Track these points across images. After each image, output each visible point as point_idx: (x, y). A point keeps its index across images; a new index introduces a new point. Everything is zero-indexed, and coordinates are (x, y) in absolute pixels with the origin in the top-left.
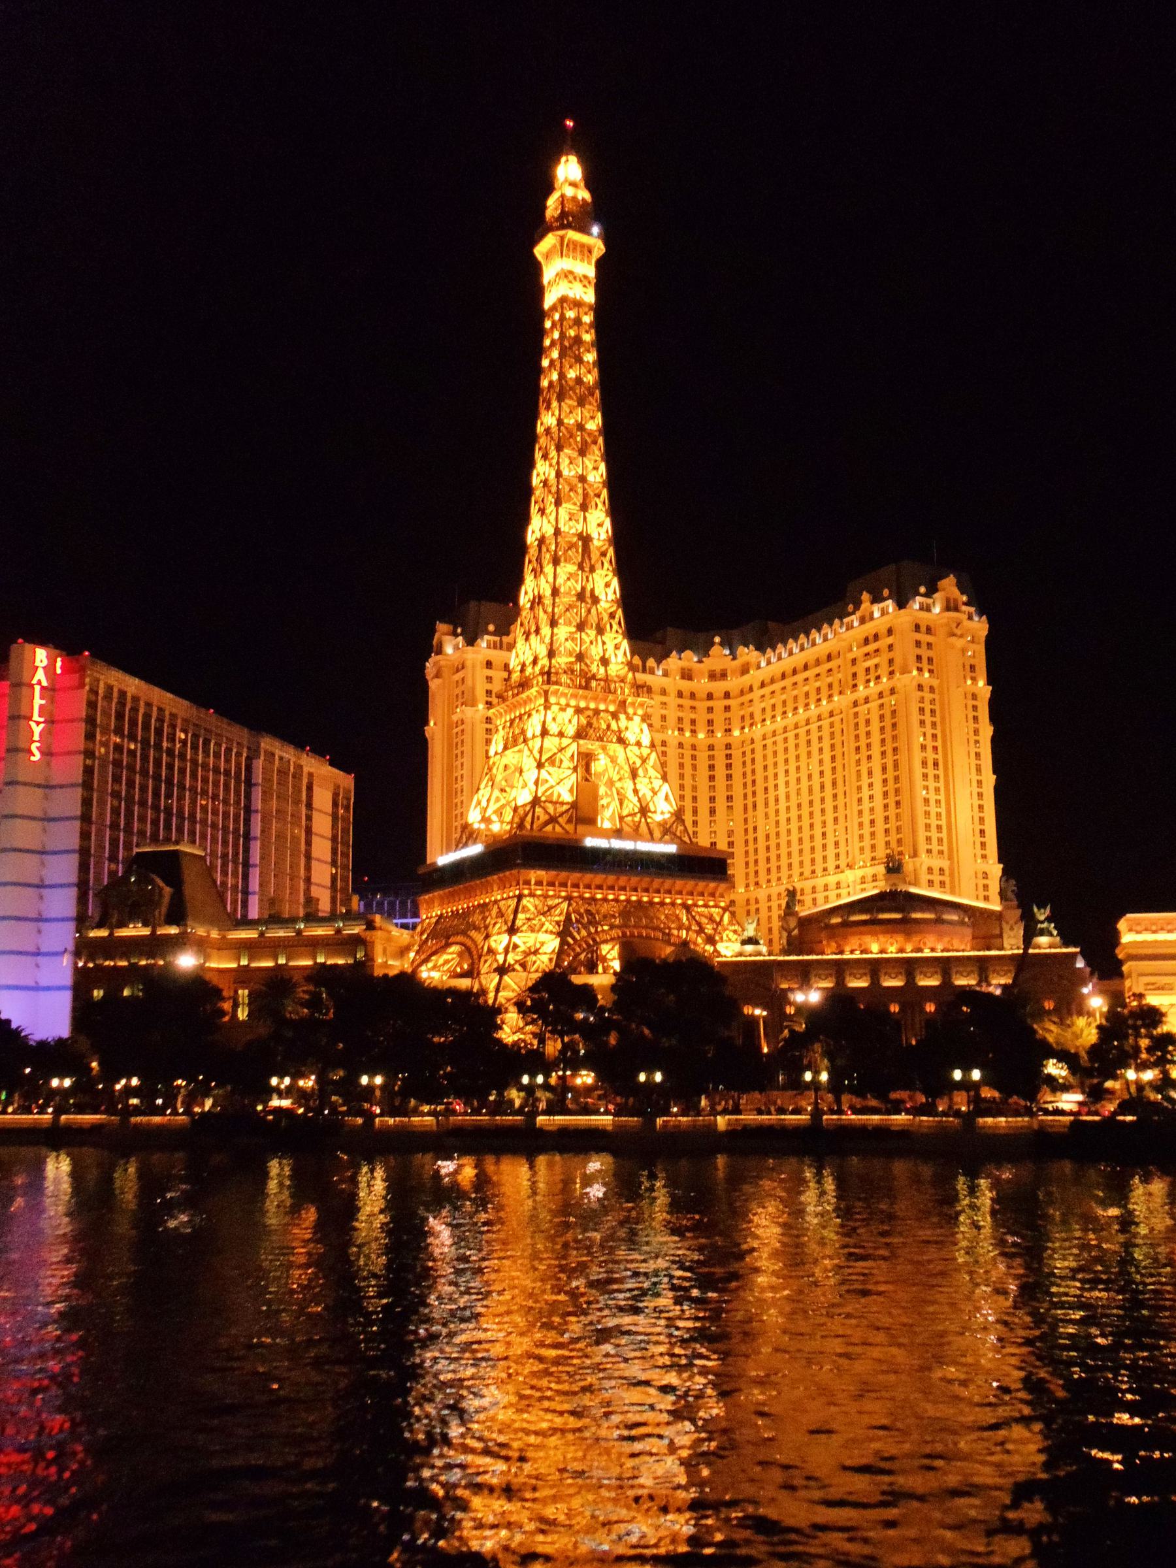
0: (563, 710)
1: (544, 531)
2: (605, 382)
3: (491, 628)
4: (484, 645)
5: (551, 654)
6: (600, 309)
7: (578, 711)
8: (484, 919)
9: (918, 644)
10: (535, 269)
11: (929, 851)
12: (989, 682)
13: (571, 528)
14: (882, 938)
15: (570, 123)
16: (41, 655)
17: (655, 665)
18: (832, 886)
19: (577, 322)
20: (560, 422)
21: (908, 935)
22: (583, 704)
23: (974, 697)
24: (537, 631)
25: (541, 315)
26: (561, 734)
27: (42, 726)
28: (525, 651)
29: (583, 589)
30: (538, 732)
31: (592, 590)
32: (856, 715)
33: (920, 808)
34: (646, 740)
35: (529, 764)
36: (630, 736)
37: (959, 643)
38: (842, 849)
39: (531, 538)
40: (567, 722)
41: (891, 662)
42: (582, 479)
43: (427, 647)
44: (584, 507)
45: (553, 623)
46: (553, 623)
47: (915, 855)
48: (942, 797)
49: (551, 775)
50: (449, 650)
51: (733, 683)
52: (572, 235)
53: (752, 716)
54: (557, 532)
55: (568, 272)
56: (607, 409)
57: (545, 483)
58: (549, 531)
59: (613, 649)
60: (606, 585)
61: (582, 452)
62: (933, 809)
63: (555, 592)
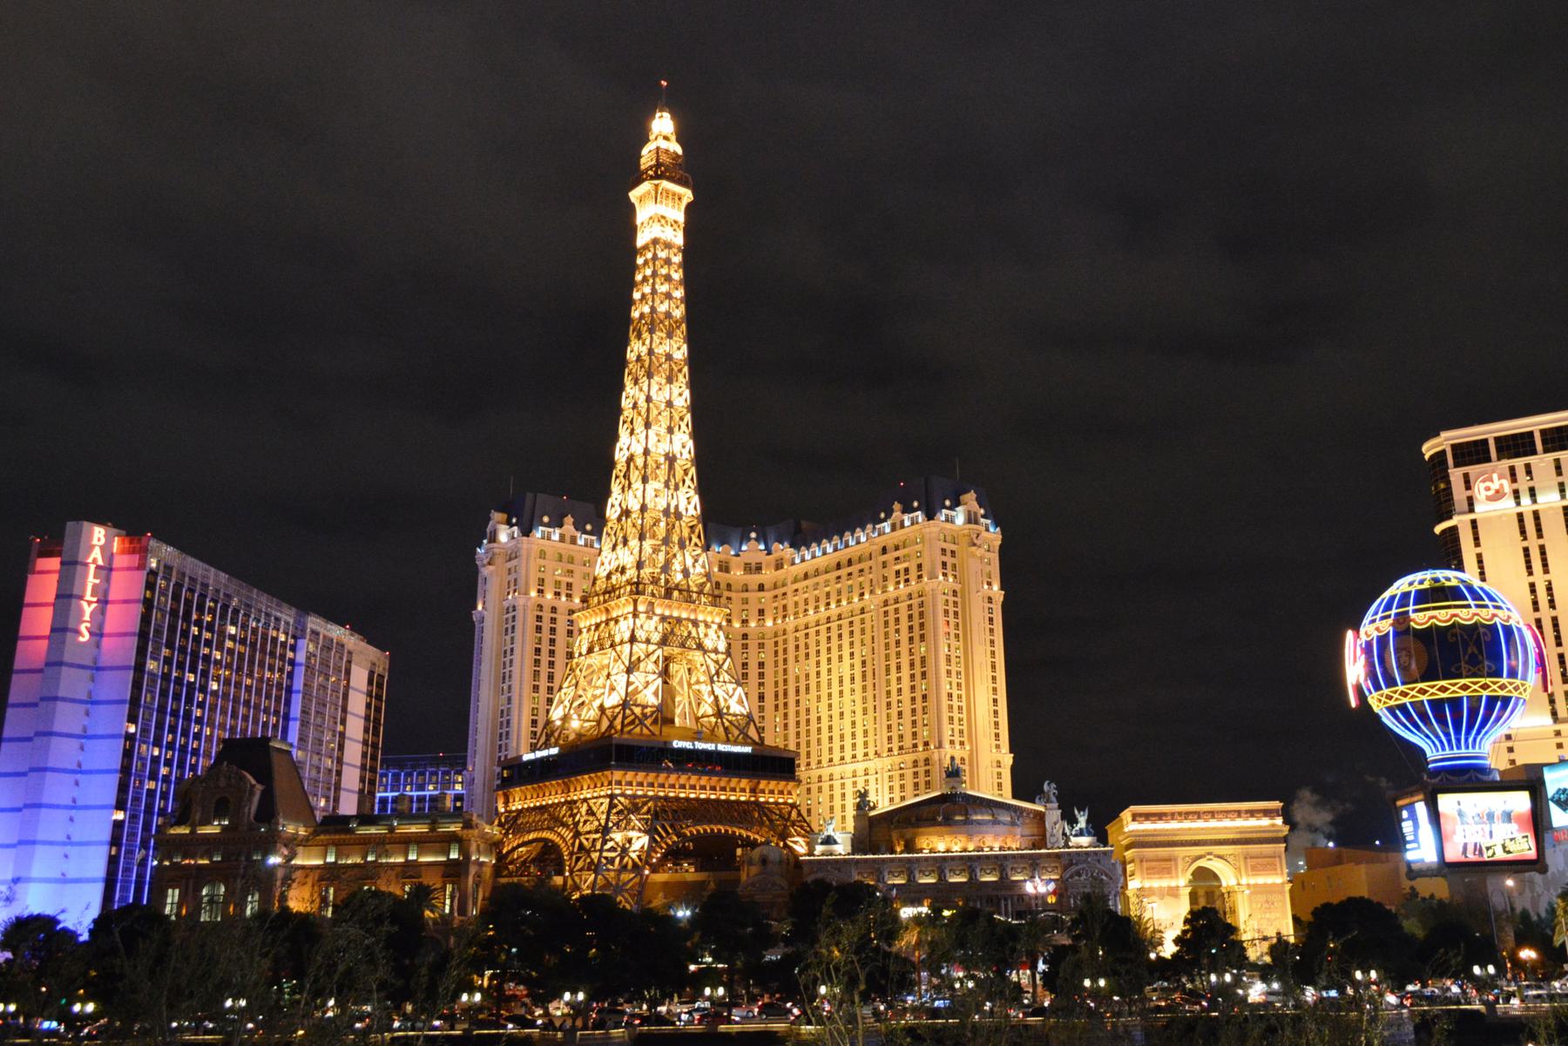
1: (632, 450)
2: (691, 317)
3: (546, 519)
4: (539, 535)
5: (639, 565)
6: (689, 251)
8: (573, 816)
9: (944, 551)
10: (631, 209)
11: (952, 742)
12: (1002, 588)
13: (659, 449)
14: (948, 838)
15: (664, 83)
18: (860, 772)
19: (668, 262)
20: (651, 352)
21: (970, 836)
22: (667, 613)
23: (990, 600)
24: (625, 542)
25: (634, 252)
26: (648, 641)
28: (613, 558)
30: (627, 636)
31: (677, 507)
32: (886, 613)
33: (945, 702)
34: (722, 646)
35: (620, 667)
36: (708, 644)
37: (979, 552)
38: (871, 739)
39: (620, 456)
40: (651, 628)
41: (920, 566)
42: (669, 404)
43: (481, 532)
44: (670, 430)
45: (642, 538)
46: (642, 538)
47: (940, 746)
48: (963, 692)
49: (638, 678)
50: (503, 537)
51: (768, 575)
52: (665, 184)
53: (785, 607)
54: (646, 452)
55: (659, 216)
56: (691, 340)
57: (635, 406)
58: (638, 450)
59: (693, 563)
60: (689, 502)
61: (670, 380)
62: (955, 703)
63: (643, 508)
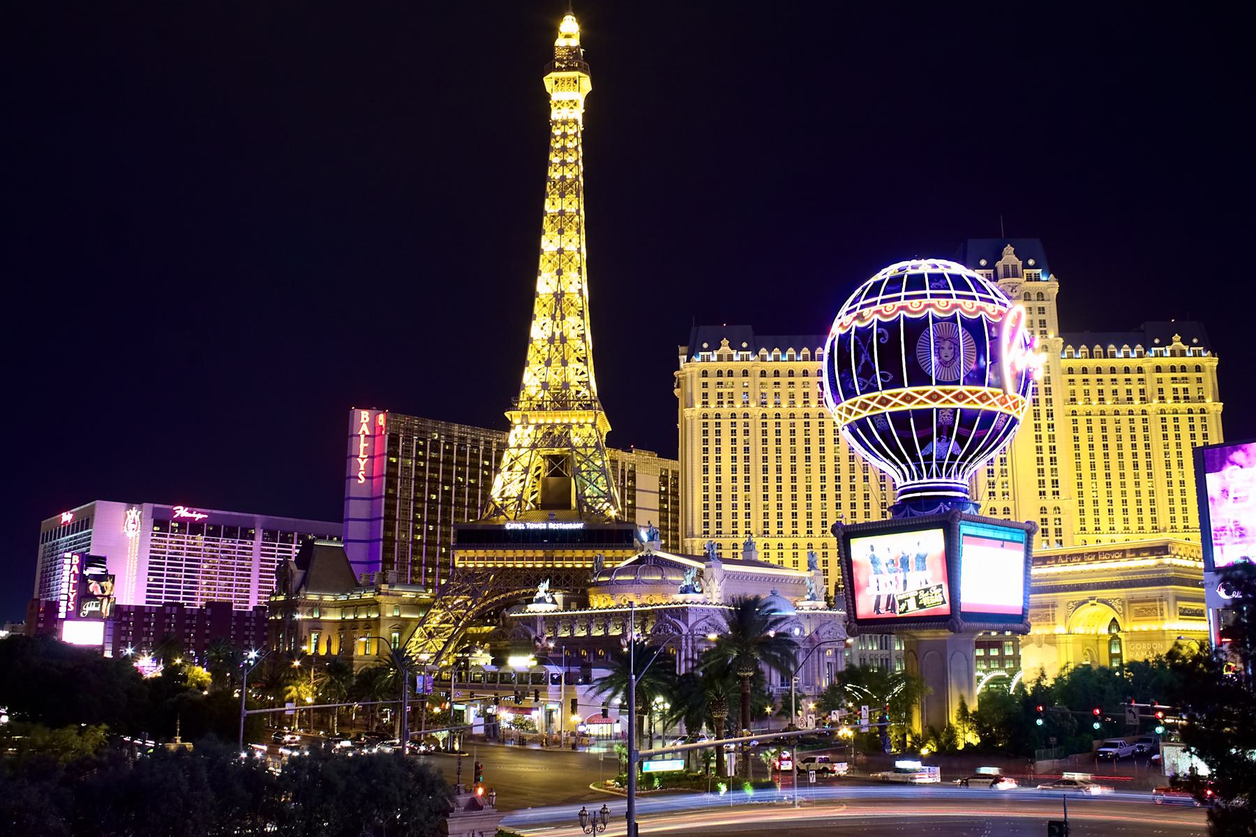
3: (705, 345)
16: (365, 415)
22: (541, 421)
29: (553, 334)
44: (560, 272)
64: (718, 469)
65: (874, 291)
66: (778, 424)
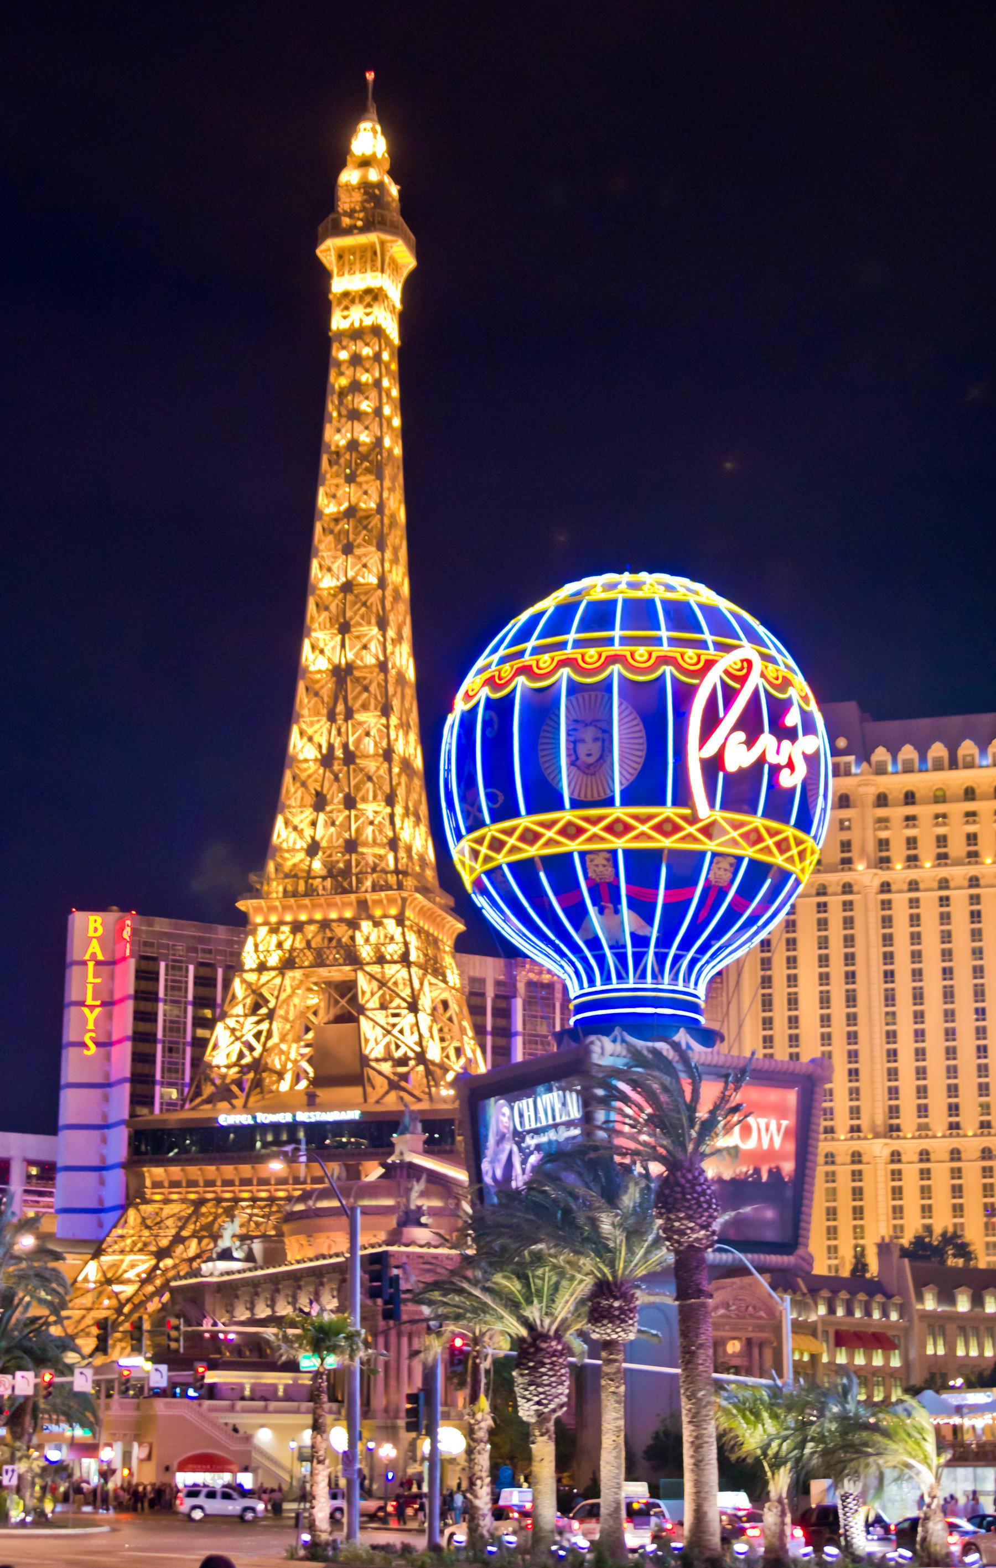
0: (274, 930)
7: (297, 927)
17: (975, 751)
27: (98, 1010)
29: (331, 747)
64: (793, 1002)
65: (524, 634)
66: (914, 903)
